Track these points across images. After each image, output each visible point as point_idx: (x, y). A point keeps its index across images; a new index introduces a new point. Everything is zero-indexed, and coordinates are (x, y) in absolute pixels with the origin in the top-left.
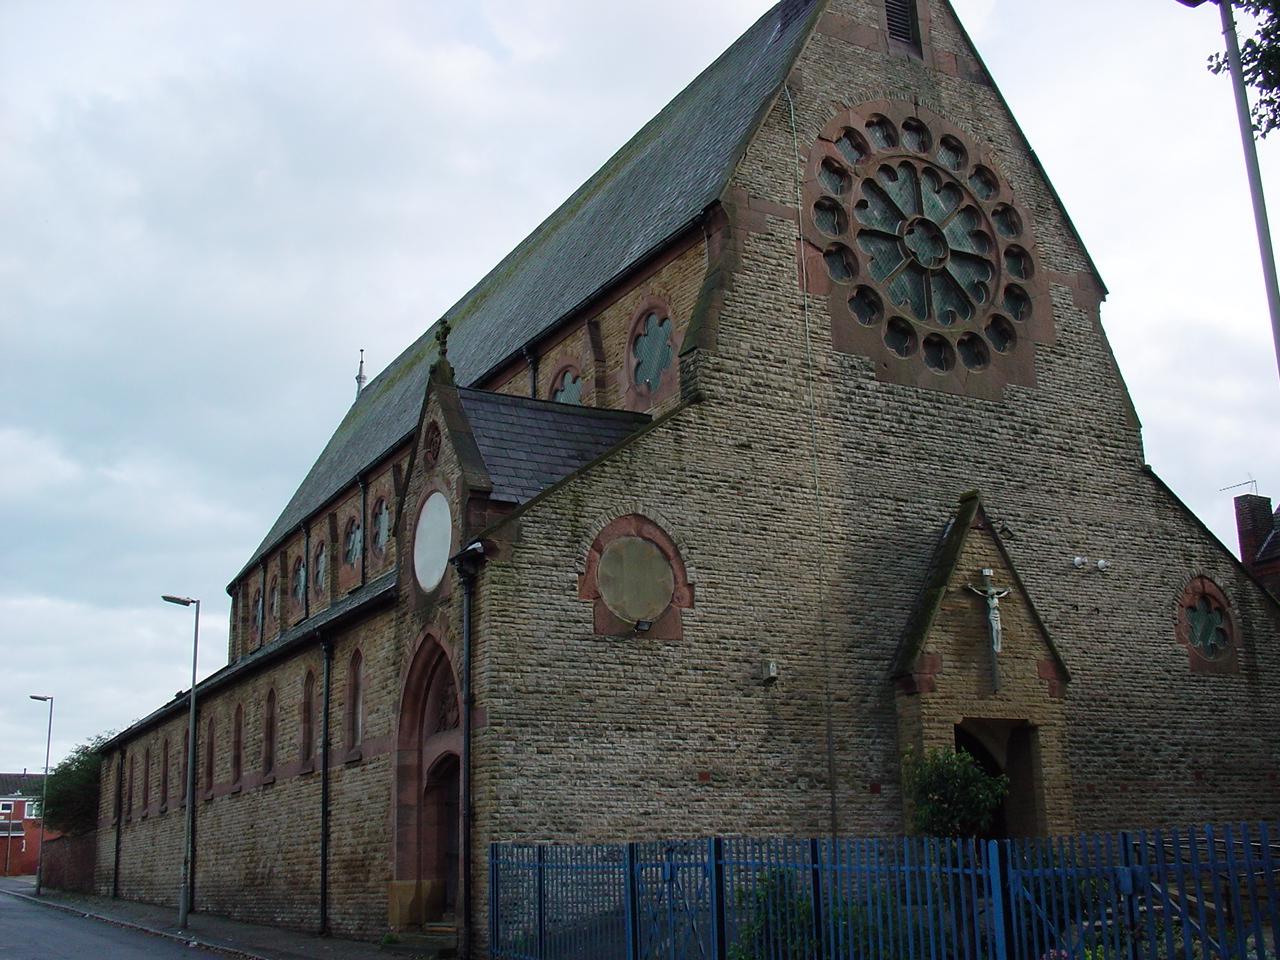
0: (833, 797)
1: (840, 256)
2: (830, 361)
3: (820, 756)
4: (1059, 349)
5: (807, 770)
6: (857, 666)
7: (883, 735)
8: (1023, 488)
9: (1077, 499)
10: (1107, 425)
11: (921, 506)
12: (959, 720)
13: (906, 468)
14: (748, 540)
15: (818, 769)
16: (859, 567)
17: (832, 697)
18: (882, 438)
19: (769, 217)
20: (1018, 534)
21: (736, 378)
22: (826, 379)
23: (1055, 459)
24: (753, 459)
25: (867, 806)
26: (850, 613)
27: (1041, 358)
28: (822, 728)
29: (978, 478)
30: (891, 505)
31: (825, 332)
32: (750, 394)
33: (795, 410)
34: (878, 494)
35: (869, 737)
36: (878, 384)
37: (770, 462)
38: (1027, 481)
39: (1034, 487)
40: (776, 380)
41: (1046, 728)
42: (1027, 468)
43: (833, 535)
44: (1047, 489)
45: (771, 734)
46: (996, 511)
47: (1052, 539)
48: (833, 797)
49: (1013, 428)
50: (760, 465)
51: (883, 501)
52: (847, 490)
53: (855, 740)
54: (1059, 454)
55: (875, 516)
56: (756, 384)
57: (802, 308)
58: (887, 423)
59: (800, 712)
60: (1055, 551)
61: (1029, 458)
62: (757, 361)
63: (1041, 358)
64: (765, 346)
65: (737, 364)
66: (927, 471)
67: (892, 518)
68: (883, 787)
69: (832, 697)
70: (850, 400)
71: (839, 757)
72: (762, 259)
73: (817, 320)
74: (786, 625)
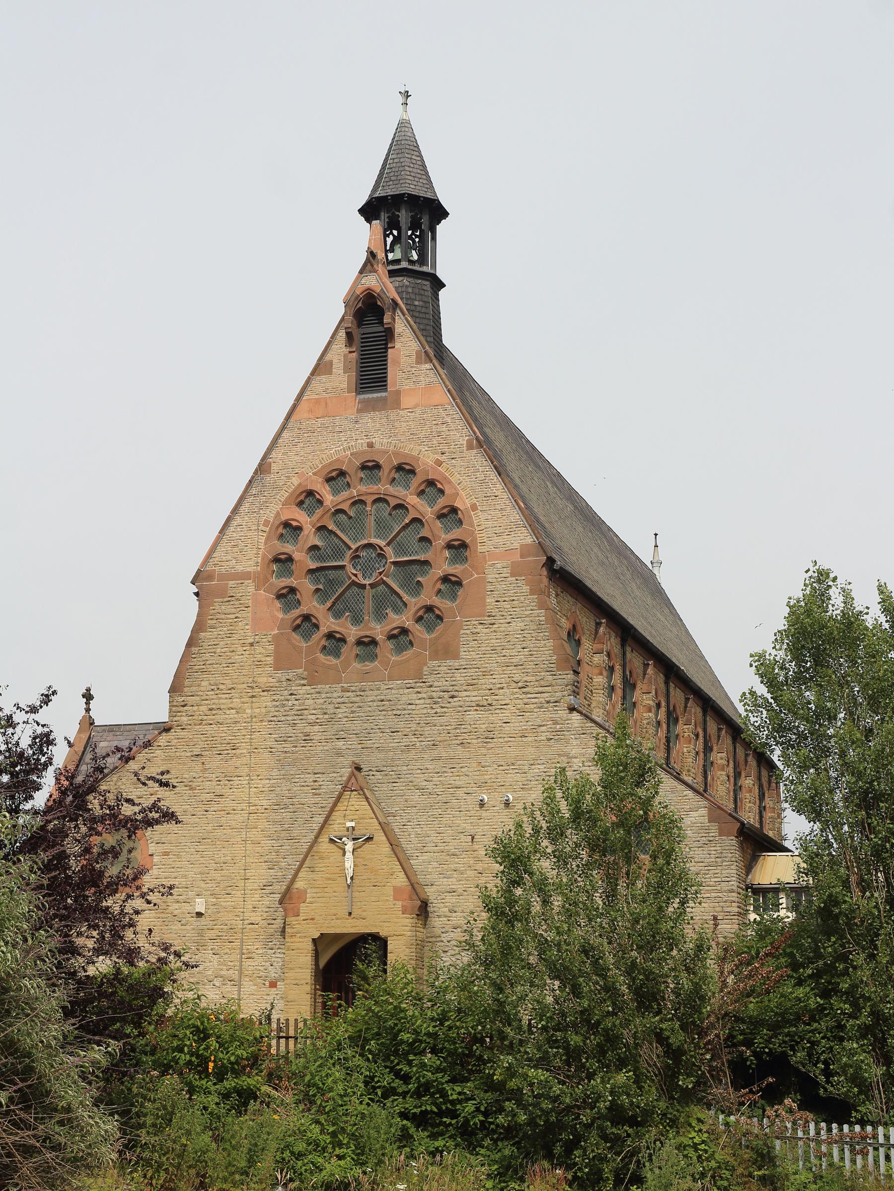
0: (239, 991)
1: (288, 596)
2: (271, 680)
3: (232, 964)
4: (489, 620)
5: (223, 973)
6: (268, 899)
7: (282, 947)
8: (434, 745)
9: (489, 745)
10: (533, 676)
11: (335, 775)
12: (316, 935)
13: (325, 748)
14: (195, 819)
15: (231, 972)
16: (279, 828)
17: (246, 922)
18: (308, 729)
19: (231, 583)
20: (425, 783)
21: (195, 708)
22: (265, 693)
23: (472, 715)
24: (203, 763)
25: (265, 997)
26: (266, 862)
27: (468, 632)
28: (237, 944)
29: (391, 745)
30: (312, 777)
31: (268, 659)
32: (205, 718)
33: (239, 722)
34: (300, 772)
35: (272, 949)
36: (309, 688)
37: (215, 763)
38: (439, 739)
39: (445, 743)
40: (224, 702)
41: (395, 937)
42: (440, 728)
43: (259, 808)
44: (459, 742)
45: (198, 950)
46: (405, 768)
47: (458, 783)
48: (239, 991)
49: (431, 698)
50: (207, 766)
51: (302, 776)
52: (275, 773)
53: (260, 951)
54: (477, 710)
55: (295, 789)
56: (210, 710)
57: (252, 645)
58: (313, 717)
59: (220, 934)
60: (460, 793)
61: (443, 720)
62: (212, 693)
63: (468, 632)
64: (220, 679)
65: (198, 698)
66: (344, 747)
67: (309, 788)
68: (279, 983)
69: (246, 922)
70: (284, 706)
71: (247, 963)
72: (223, 616)
73: (265, 650)
74: (217, 875)
